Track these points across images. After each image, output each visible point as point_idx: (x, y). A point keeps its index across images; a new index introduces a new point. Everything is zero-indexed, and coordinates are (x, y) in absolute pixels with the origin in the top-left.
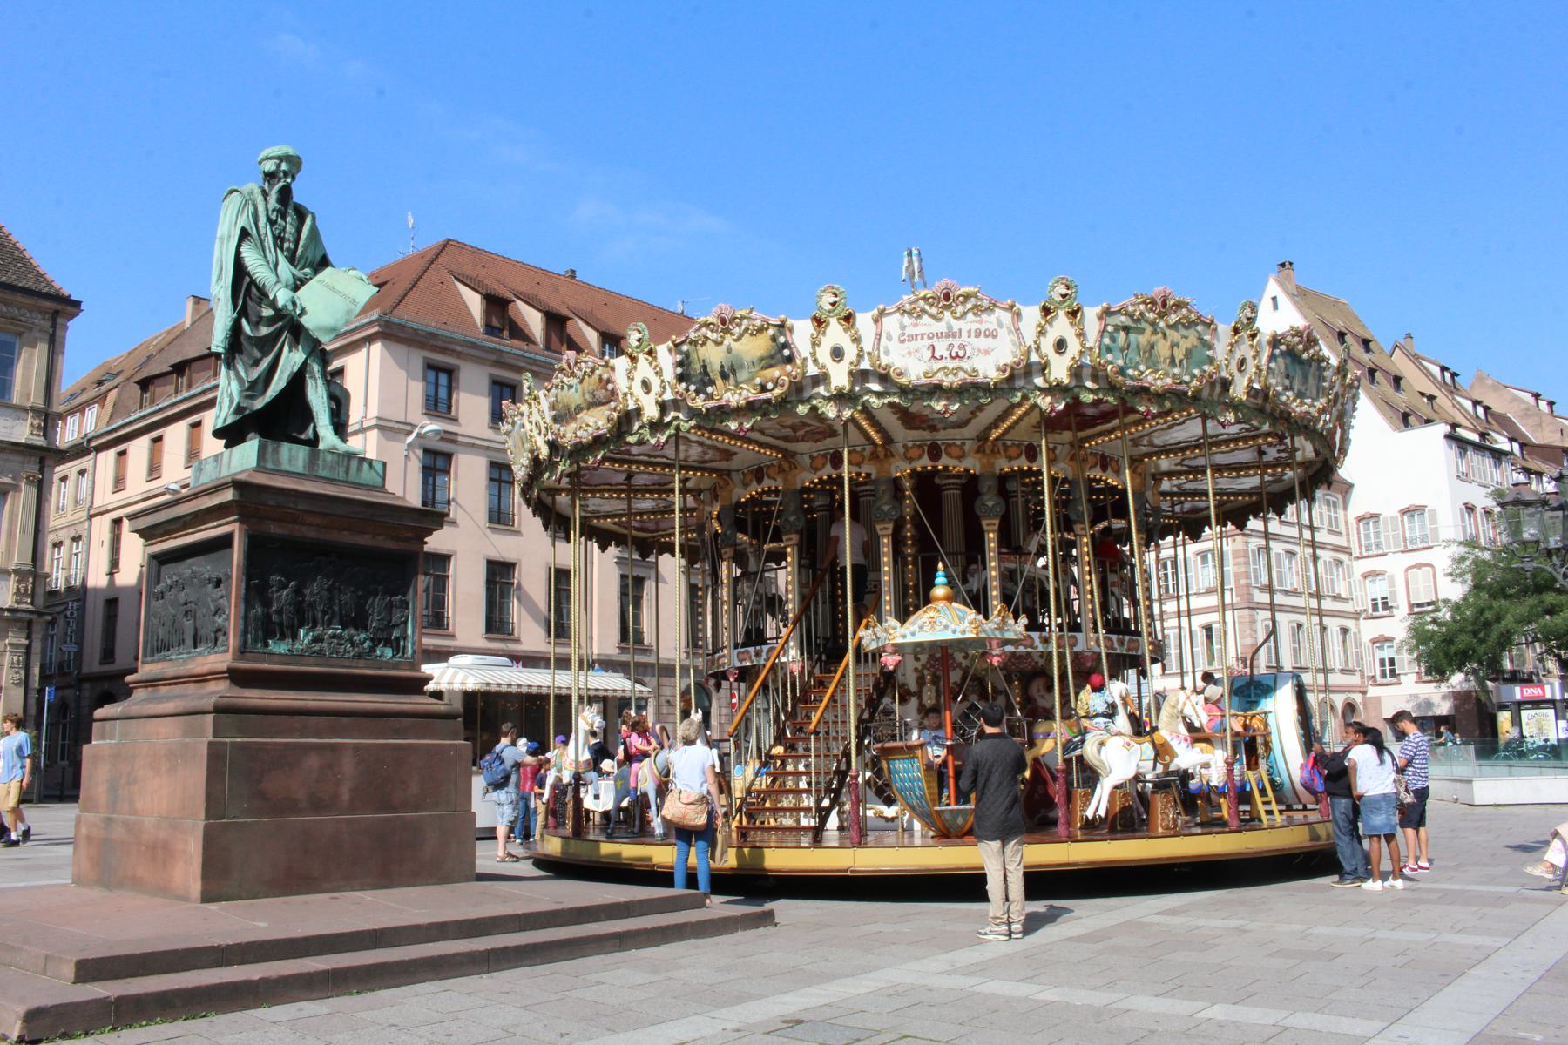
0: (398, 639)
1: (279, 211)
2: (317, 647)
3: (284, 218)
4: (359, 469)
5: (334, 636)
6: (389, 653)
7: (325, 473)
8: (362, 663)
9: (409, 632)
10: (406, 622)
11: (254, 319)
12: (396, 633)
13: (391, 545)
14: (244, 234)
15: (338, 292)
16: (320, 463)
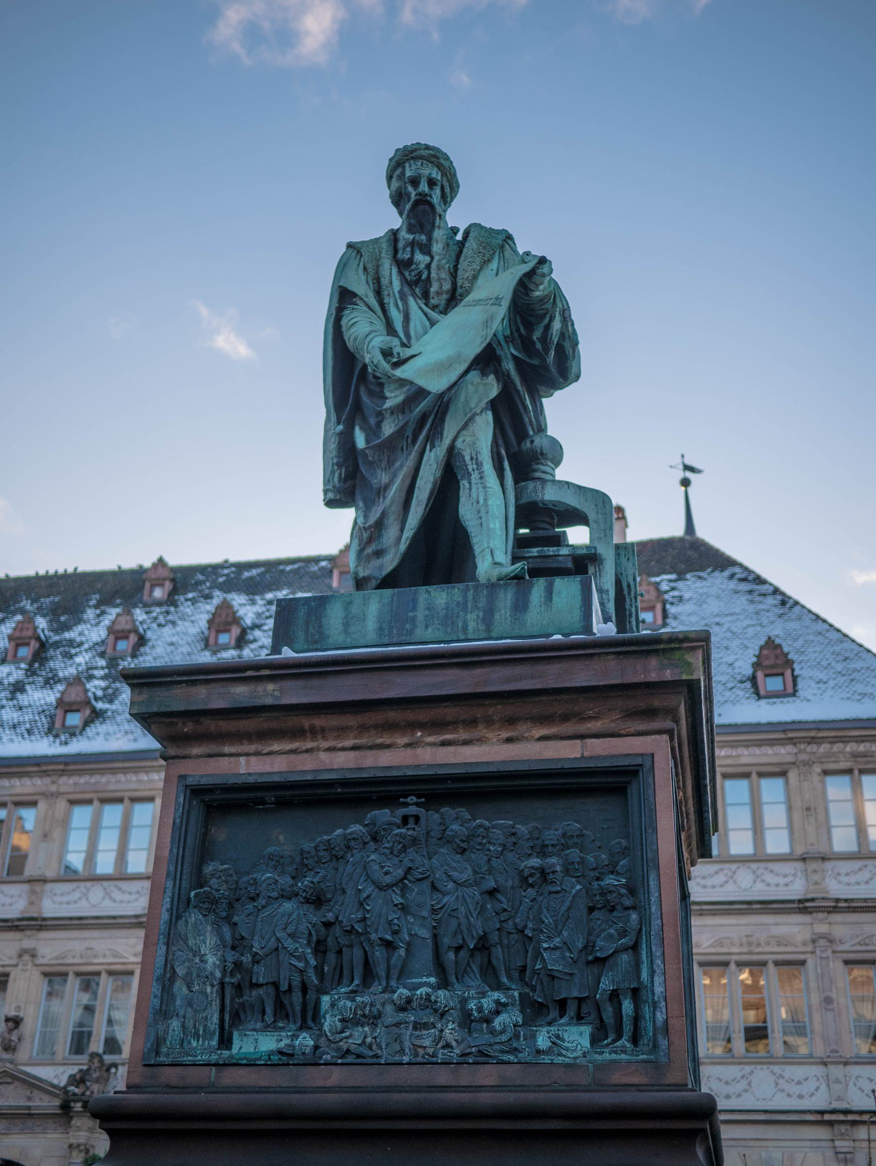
0: (615, 996)
1: (412, 244)
2: (357, 1036)
3: (426, 249)
4: (521, 606)
5: (405, 1006)
6: (577, 1038)
7: (429, 634)
8: (487, 1075)
9: (644, 975)
10: (635, 947)
11: (373, 421)
12: (606, 984)
13: (565, 752)
14: (344, 298)
15: (477, 303)
16: (420, 614)
